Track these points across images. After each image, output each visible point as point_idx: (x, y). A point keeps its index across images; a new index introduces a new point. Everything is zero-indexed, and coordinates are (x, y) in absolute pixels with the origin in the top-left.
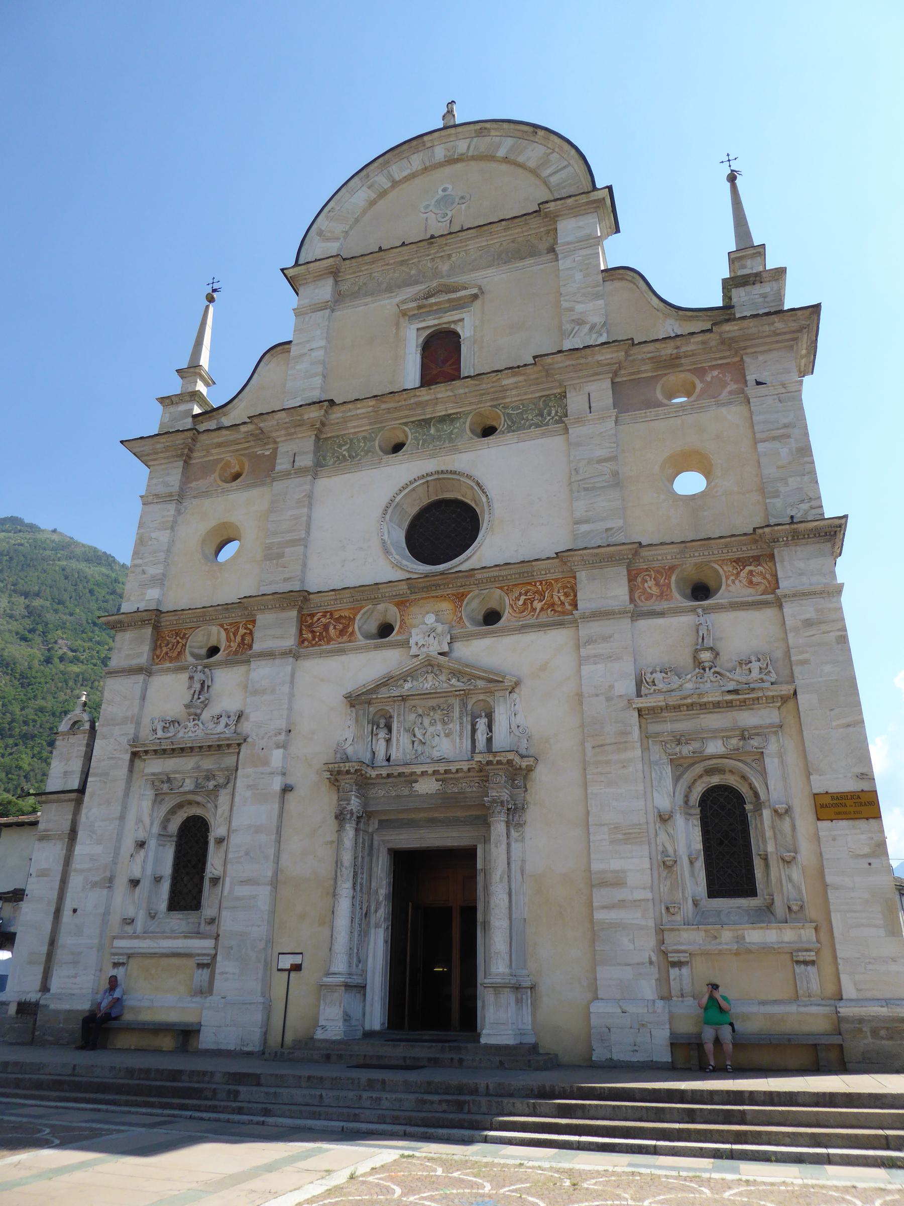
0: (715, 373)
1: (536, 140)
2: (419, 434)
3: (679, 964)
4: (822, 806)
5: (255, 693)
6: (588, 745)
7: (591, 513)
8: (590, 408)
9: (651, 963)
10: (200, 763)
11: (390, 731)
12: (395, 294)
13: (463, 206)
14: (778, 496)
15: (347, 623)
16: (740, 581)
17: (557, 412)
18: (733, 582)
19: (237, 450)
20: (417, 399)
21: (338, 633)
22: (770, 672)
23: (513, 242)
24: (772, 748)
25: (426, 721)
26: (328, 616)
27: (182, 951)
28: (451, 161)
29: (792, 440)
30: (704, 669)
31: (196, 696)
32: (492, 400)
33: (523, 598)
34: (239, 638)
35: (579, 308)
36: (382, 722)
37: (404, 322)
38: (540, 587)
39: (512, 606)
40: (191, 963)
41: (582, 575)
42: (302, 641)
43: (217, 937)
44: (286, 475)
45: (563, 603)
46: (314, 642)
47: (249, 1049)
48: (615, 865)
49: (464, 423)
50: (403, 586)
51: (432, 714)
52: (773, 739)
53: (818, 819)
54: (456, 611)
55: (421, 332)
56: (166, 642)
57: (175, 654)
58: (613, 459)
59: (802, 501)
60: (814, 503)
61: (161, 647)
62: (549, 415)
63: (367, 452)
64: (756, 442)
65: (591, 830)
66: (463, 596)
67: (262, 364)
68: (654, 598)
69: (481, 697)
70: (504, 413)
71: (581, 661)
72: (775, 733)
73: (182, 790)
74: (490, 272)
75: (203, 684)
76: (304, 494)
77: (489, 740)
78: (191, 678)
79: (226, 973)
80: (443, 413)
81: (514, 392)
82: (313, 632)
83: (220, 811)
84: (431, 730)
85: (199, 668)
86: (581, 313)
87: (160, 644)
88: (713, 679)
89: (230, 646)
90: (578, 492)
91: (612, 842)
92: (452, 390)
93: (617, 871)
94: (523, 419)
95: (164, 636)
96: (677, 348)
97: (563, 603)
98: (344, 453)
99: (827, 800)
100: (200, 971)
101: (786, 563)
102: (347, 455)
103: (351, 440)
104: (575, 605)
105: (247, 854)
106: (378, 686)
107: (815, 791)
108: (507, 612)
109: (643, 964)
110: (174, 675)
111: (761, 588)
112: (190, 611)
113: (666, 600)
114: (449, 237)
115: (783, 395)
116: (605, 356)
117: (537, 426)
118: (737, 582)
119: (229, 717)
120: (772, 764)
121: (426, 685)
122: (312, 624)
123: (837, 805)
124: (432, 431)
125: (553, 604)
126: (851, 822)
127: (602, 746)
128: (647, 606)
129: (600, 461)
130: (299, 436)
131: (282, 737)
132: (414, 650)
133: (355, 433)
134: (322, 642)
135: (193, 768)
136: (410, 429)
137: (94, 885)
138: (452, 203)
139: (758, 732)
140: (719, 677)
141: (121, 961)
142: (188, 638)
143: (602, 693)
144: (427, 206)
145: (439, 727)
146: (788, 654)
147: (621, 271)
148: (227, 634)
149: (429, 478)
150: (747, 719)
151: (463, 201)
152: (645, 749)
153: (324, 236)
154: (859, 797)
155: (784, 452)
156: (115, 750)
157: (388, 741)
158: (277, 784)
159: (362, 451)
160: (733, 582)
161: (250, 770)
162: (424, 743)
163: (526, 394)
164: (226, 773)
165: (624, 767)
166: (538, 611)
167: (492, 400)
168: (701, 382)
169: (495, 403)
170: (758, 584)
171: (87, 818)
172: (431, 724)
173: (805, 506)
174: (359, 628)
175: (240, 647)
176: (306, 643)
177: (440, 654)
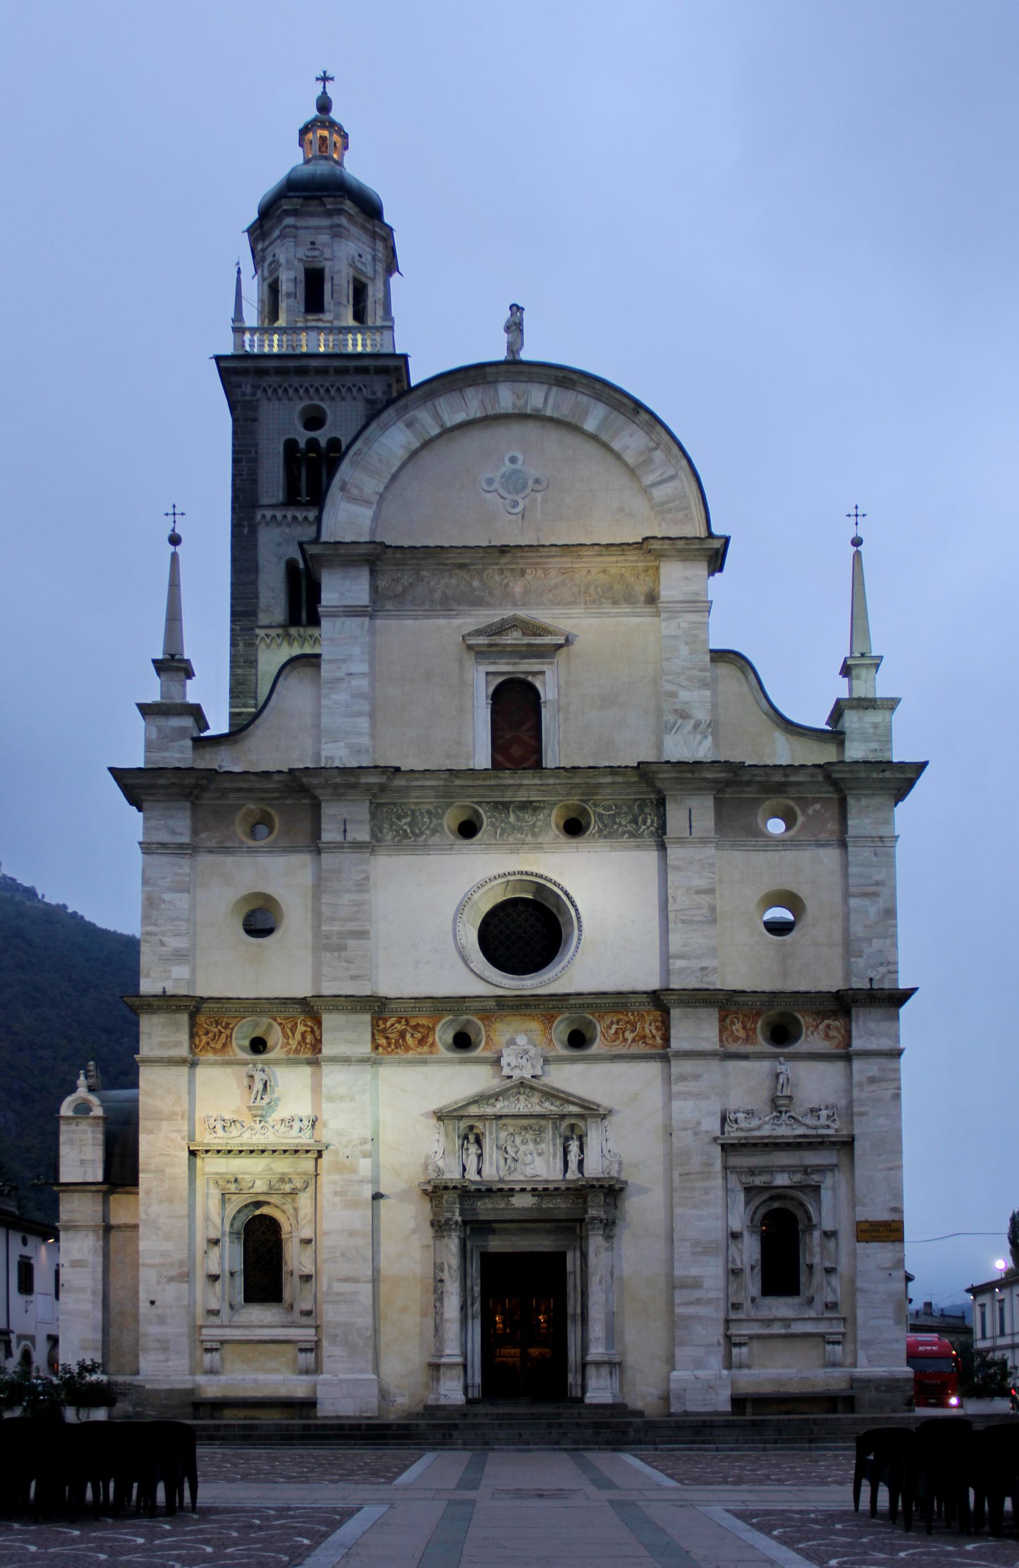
0: (818, 807)
1: (636, 421)
3: (740, 1345)
4: (862, 1231)
6: (676, 1174)
8: (690, 827)
9: (719, 1344)
10: (272, 1166)
12: (454, 613)
13: (539, 496)
14: (861, 956)
16: (818, 1033)
17: (653, 822)
18: (812, 1033)
19: (263, 799)
21: (416, 1042)
22: (835, 1120)
23: (604, 571)
24: (828, 1182)
25: (518, 1140)
28: (522, 417)
29: (881, 900)
30: (780, 1112)
31: (259, 1097)
32: (582, 794)
33: (614, 1027)
34: (298, 1036)
35: (684, 695)
36: (472, 1138)
37: (469, 659)
38: (632, 1017)
41: (675, 1013)
42: (376, 1047)
43: (317, 1327)
44: (338, 847)
45: (654, 1037)
46: (389, 1049)
47: (369, 1414)
48: (694, 1271)
49: (549, 815)
50: (492, 1003)
51: (523, 1133)
52: (829, 1175)
53: (858, 1241)
54: (545, 1033)
55: (490, 678)
56: (203, 1030)
57: (219, 1046)
58: (711, 891)
59: (882, 964)
60: (891, 968)
61: (199, 1036)
62: (645, 824)
63: (434, 832)
64: (847, 896)
65: (676, 1243)
66: (552, 1017)
67: (281, 679)
68: (741, 1040)
69: (573, 1121)
70: (594, 812)
71: (669, 1097)
72: (832, 1170)
73: (252, 1191)
74: (578, 611)
76: (363, 876)
77: (581, 1163)
79: (335, 1356)
81: (608, 791)
82: (387, 1038)
85: (260, 1066)
86: (686, 703)
88: (788, 1122)
89: (288, 1043)
90: (675, 923)
91: (694, 1254)
92: (540, 778)
93: (695, 1277)
94: (616, 823)
95: (200, 1022)
96: (786, 776)
97: (654, 1037)
98: (405, 827)
99: (866, 1227)
101: (861, 1023)
102: (409, 831)
103: (413, 812)
104: (666, 1039)
106: (469, 1104)
107: (858, 1219)
109: (712, 1345)
111: (835, 1042)
113: (752, 1044)
114: (526, 549)
115: (879, 849)
117: (632, 835)
118: (815, 1033)
119: (301, 1121)
120: (826, 1195)
121: (518, 1106)
122: (384, 1030)
123: (873, 1231)
124: (512, 819)
125: (644, 1037)
126: (881, 1244)
127: (688, 1174)
128: (734, 1048)
129: (699, 892)
132: (506, 1071)
133: (416, 804)
134: (399, 1051)
135: (264, 1170)
136: (486, 812)
137: (171, 1279)
138: (524, 487)
139: (821, 1169)
140: (793, 1121)
141: (214, 1347)
142: (232, 1029)
144: (490, 481)
145: (531, 1146)
146: (850, 1103)
147: (731, 656)
149: (511, 878)
150: (812, 1158)
151: (538, 487)
152: (725, 1178)
153: (349, 491)
154: (890, 1225)
155: (872, 910)
156: (168, 1147)
157: (480, 1156)
159: (427, 829)
160: (812, 1033)
161: (336, 1177)
162: (516, 1161)
163: (621, 794)
164: (304, 1177)
166: (629, 1041)
169: (585, 798)
170: (833, 1038)
171: (147, 1215)
172: (524, 1142)
173: (883, 970)
174: (440, 1038)
175: (301, 1046)
176: (381, 1050)
177: (532, 1077)
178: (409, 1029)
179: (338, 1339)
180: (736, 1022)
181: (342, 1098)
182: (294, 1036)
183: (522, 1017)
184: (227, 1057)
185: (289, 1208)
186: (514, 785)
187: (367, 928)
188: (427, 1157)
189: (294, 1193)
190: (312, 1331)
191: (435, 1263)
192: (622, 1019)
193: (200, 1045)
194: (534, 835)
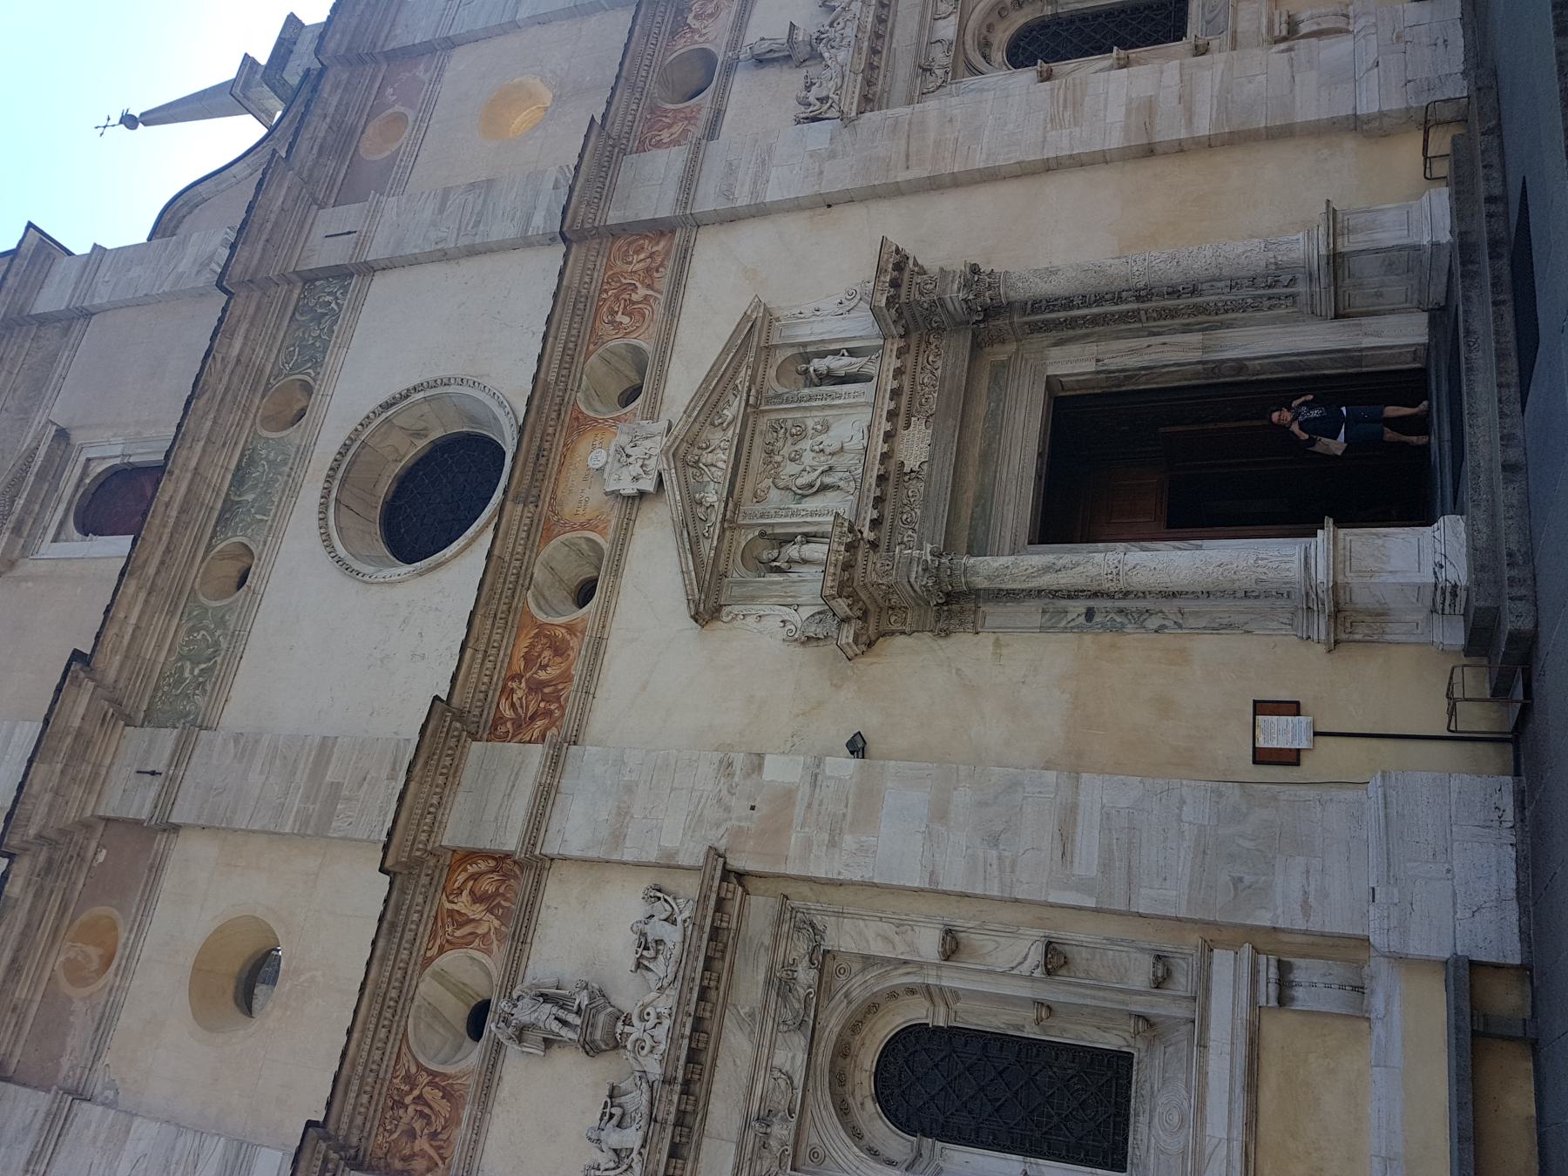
2: (243, 520)
5: (618, 837)
6: (902, 176)
7: (518, 214)
11: (789, 539)
15: (544, 641)
20: (176, 506)
21: (558, 659)
26: (515, 685)
27: (1242, 1049)
32: (253, 390)
34: (477, 911)
39: (626, 334)
40: (1276, 1029)
45: (651, 256)
46: (557, 713)
47: (1508, 802)
48: (1116, 115)
54: (601, 429)
57: (443, 1107)
61: (413, 1156)
63: (222, 623)
66: (577, 419)
73: (799, 1080)
75: (546, 998)
77: (852, 352)
78: (521, 1034)
80: (229, 477)
82: (533, 718)
83: (877, 948)
84: (808, 458)
87: (404, 1159)
93: (1128, 112)
98: (196, 672)
100: (1299, 992)
102: (203, 666)
103: (181, 658)
105: (994, 840)
108: (634, 342)
110: (497, 1110)
112: (356, 1035)
116: (277, 196)
125: (648, 270)
127: (907, 156)
130: (107, 762)
131: (739, 759)
134: (564, 694)
142: (419, 1066)
143: (819, 167)
145: (806, 444)
148: (453, 945)
149: (334, 494)
158: (844, 766)
159: (212, 634)
161: (795, 838)
164: (785, 927)
165: (951, 121)
167: (253, 390)
168: (393, 106)
175: (499, 905)
178: (528, 675)
179: (1248, 879)
180: (658, 138)
181: (623, 813)
182: (473, 920)
183: (564, 470)
184: (472, 1090)
185: (860, 986)
186: (192, 481)
187: (318, 739)
188: (790, 640)
189: (822, 959)
190: (1223, 962)
191: (1043, 630)
192: (610, 308)
193: (431, 1158)
194: (285, 462)
